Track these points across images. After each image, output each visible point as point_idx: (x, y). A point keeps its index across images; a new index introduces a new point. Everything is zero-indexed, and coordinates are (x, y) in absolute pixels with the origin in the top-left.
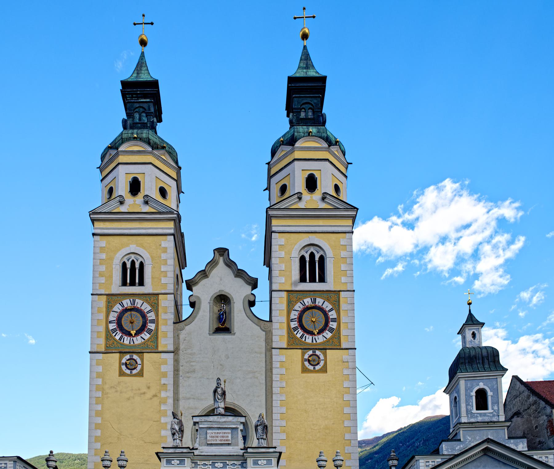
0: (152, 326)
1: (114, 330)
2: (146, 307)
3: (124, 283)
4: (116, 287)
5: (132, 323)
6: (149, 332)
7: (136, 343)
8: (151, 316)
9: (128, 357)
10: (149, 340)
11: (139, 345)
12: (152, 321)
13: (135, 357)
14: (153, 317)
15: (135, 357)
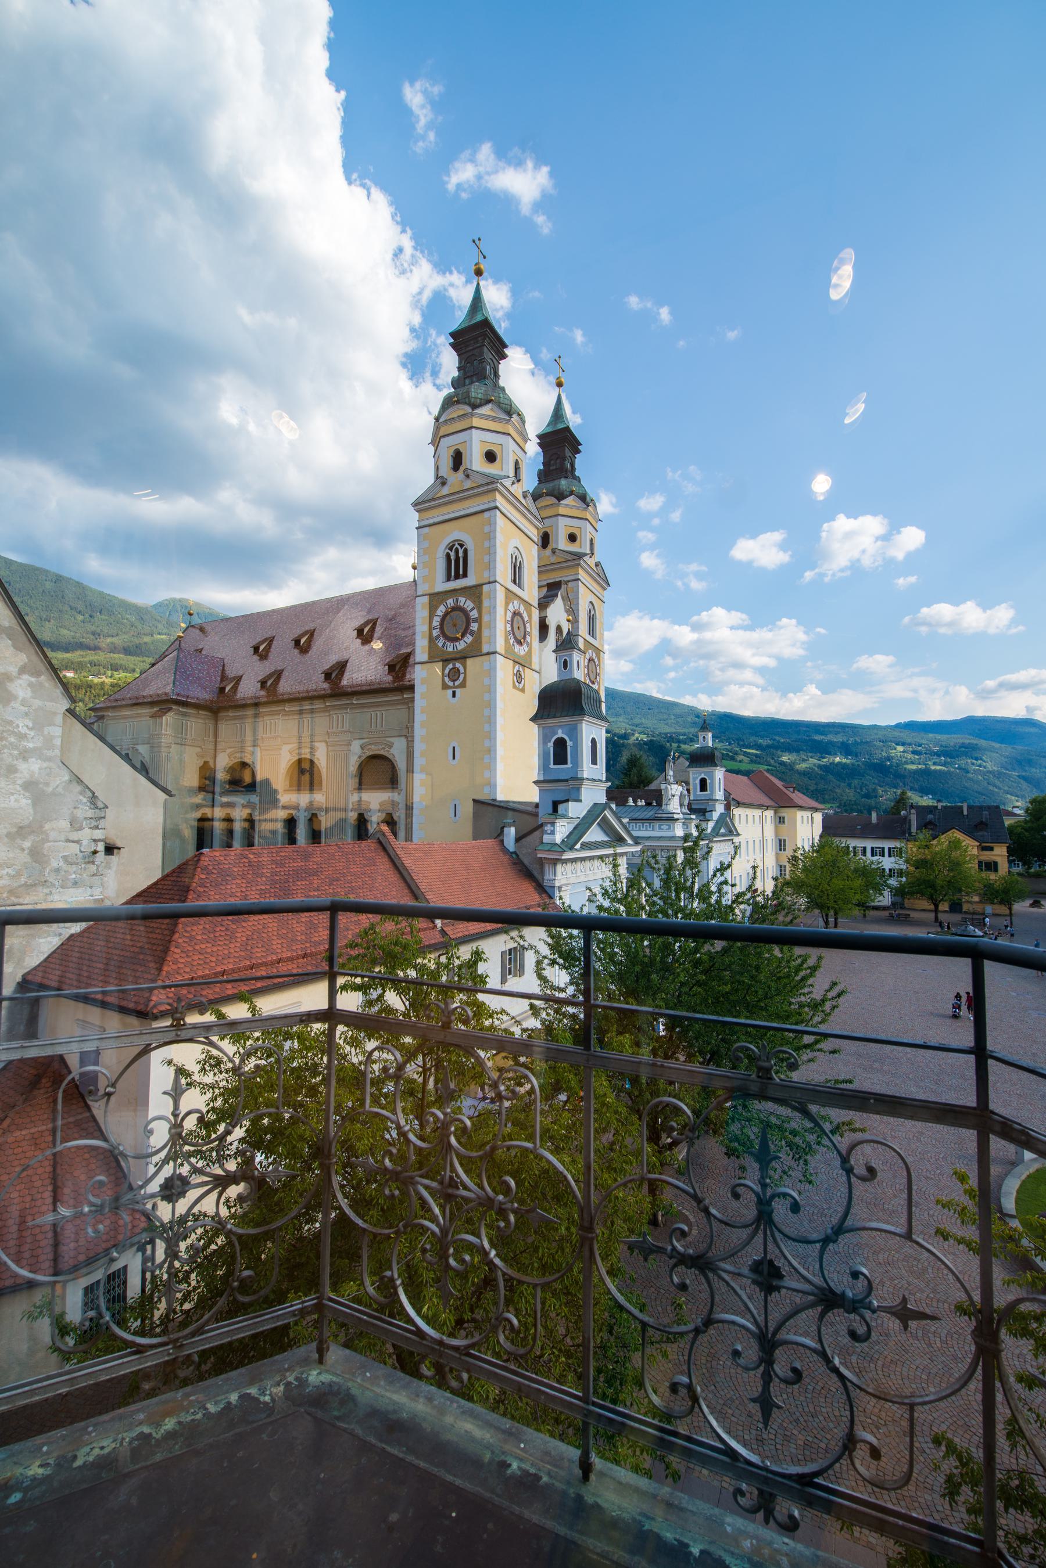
0: (474, 626)
1: (437, 637)
2: (469, 605)
3: (449, 579)
4: (441, 585)
5: (455, 625)
6: (472, 633)
7: (459, 648)
8: (474, 614)
9: (451, 666)
10: (472, 643)
11: (463, 650)
12: (475, 620)
13: (458, 665)
14: (476, 616)
15: (458, 665)
